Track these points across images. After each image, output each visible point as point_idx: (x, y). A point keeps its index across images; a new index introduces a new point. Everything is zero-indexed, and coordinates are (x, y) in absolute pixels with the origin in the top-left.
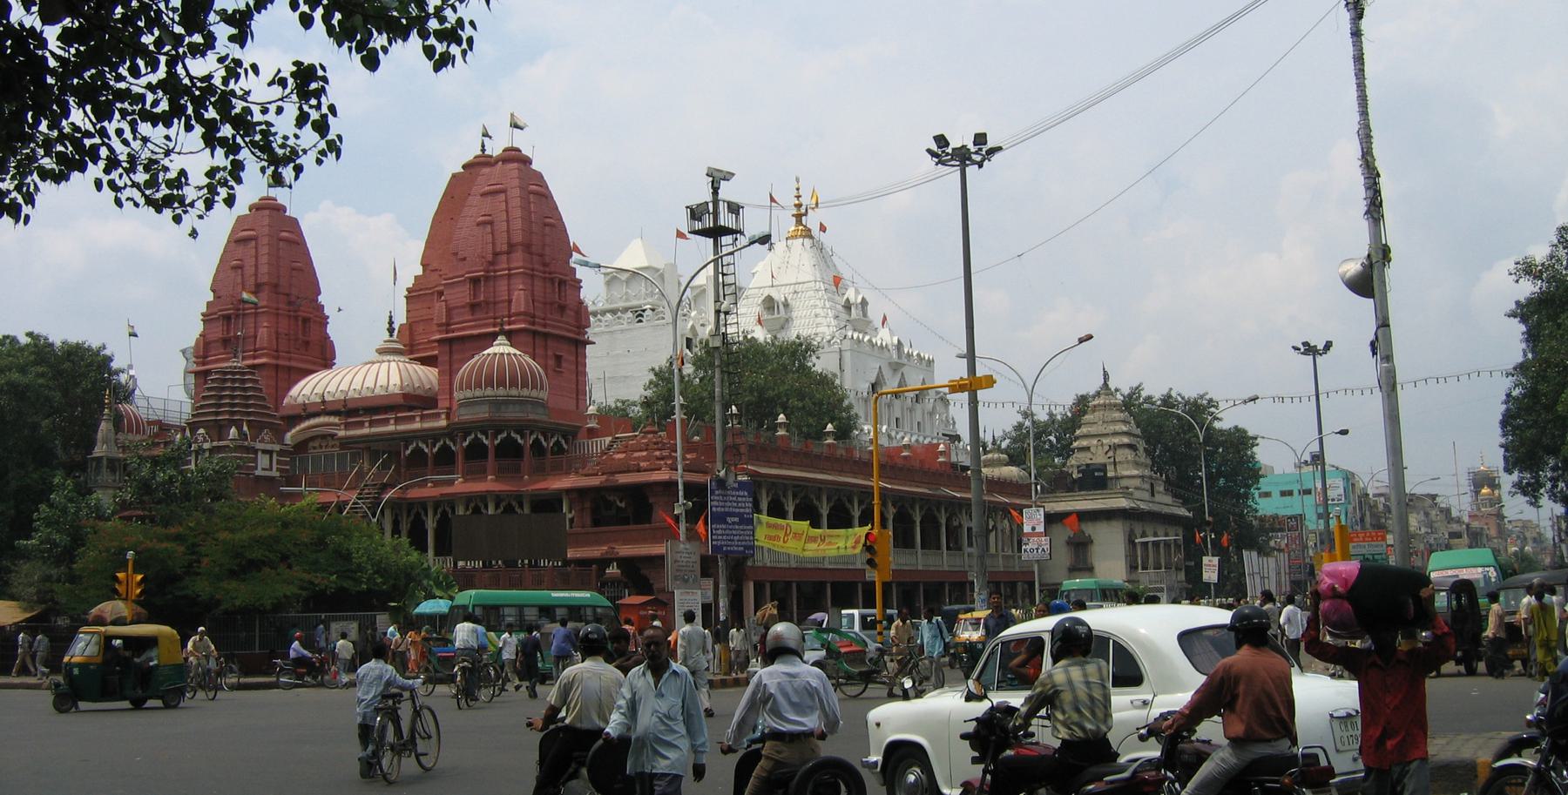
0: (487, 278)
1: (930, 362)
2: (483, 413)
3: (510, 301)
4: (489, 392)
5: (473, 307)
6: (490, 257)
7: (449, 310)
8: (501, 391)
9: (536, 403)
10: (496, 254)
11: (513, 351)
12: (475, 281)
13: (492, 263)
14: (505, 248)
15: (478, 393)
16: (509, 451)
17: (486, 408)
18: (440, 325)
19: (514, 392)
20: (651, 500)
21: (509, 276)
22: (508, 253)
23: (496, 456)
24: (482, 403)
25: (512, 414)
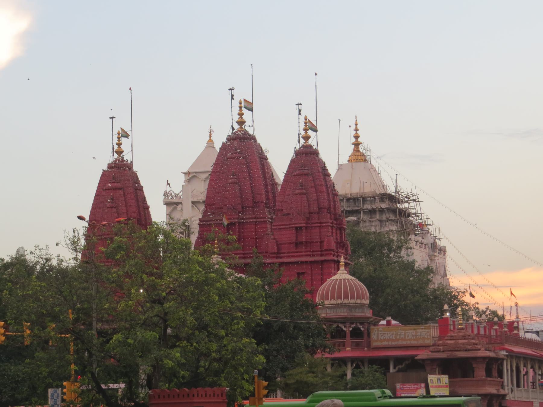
0: (306, 227)
1: (445, 252)
2: (343, 313)
3: (322, 242)
4: (346, 301)
5: (297, 244)
6: (308, 215)
7: (278, 245)
8: (353, 301)
9: (361, 306)
10: (310, 213)
11: (350, 277)
12: (298, 229)
13: (308, 219)
14: (316, 210)
15: (339, 301)
16: (356, 333)
17: (345, 310)
18: (272, 253)
19: (359, 301)
20: (474, 366)
21: (320, 226)
22: (318, 213)
23: (351, 337)
24: (342, 307)
25: (358, 314)
